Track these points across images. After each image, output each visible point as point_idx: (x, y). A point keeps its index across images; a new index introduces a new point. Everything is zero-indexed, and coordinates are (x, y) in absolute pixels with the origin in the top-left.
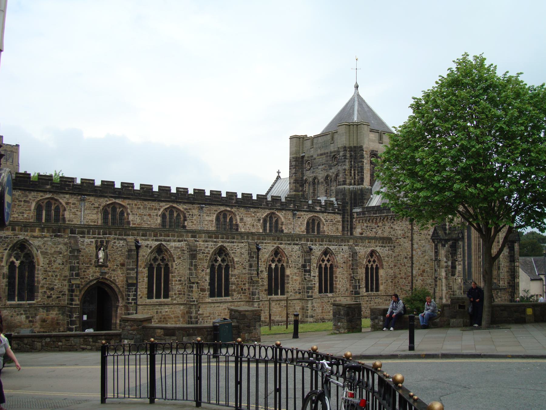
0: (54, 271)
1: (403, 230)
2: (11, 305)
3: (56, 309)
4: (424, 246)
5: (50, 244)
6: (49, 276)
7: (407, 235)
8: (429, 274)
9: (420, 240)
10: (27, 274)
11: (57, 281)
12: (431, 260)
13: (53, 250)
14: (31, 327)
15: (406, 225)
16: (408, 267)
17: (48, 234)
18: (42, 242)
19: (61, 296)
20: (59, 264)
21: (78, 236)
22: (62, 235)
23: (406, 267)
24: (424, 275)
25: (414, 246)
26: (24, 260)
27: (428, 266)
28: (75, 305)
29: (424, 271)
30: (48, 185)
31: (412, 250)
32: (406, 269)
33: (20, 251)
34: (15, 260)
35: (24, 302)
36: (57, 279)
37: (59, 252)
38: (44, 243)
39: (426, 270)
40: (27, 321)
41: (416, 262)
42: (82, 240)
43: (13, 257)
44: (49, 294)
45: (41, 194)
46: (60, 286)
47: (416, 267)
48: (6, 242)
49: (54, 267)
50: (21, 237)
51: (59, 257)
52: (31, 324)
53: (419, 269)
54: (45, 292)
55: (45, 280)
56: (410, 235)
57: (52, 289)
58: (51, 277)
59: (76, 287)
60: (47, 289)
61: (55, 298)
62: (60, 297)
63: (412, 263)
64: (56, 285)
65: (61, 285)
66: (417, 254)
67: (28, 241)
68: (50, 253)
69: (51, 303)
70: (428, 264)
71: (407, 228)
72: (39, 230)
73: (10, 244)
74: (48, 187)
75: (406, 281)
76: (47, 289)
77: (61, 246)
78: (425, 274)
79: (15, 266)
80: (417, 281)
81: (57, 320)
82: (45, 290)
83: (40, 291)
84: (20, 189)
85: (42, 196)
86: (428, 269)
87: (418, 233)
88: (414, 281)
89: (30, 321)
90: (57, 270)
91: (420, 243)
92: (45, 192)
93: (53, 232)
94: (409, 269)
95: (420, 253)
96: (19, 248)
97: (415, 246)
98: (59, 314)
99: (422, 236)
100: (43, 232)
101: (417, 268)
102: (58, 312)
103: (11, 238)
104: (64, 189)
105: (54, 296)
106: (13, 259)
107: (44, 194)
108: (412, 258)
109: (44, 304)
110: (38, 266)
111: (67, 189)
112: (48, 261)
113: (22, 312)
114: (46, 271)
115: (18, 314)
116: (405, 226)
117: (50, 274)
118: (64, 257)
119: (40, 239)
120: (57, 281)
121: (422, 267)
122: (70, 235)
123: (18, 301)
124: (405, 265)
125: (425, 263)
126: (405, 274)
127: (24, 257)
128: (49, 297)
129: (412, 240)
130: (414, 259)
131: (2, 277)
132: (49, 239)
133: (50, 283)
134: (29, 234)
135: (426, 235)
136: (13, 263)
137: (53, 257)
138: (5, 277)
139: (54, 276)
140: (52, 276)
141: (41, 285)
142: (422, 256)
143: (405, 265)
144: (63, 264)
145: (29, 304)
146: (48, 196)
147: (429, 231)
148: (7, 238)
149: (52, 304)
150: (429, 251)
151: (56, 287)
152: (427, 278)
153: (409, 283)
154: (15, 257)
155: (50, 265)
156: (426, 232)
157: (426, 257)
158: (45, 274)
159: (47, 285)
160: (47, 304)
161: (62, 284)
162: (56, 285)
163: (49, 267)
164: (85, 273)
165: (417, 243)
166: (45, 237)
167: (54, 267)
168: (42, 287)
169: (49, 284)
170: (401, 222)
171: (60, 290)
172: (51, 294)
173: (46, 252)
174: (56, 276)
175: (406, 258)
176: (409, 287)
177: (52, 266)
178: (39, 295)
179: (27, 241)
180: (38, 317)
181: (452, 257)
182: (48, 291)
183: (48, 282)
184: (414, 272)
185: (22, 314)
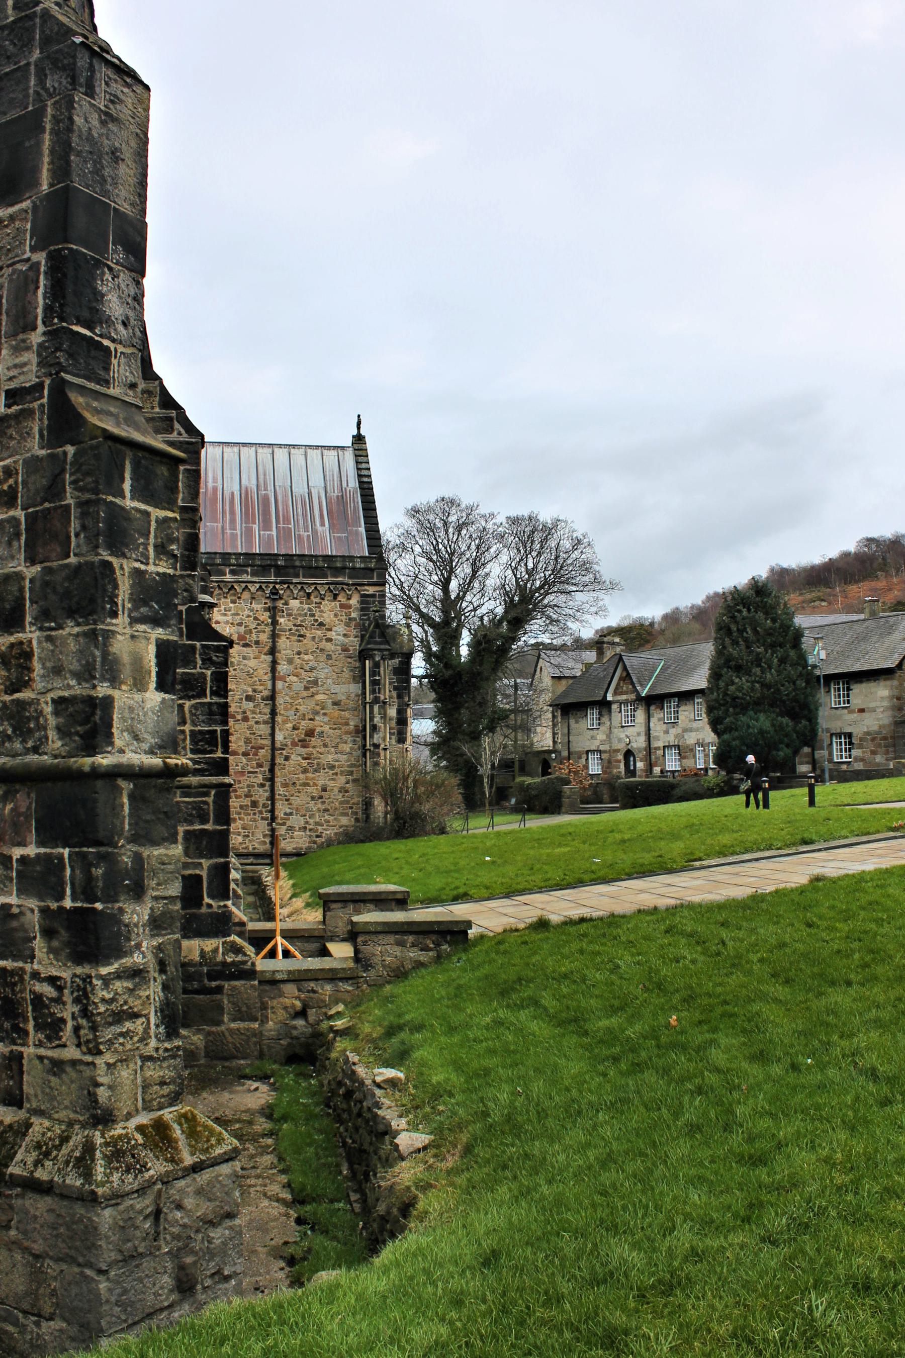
1: (240, 624)
4: (312, 669)
7: (254, 637)
8: (328, 740)
9: (299, 653)
12: (335, 703)
15: (252, 610)
16: (257, 723)
23: (252, 722)
24: (313, 743)
25: (279, 668)
27: (326, 719)
29: (310, 733)
31: (274, 679)
32: (250, 728)
39: (318, 729)
41: (286, 709)
47: (285, 722)
53: (295, 728)
56: (264, 637)
63: (273, 713)
66: (290, 687)
70: (325, 714)
71: (256, 619)
75: (249, 760)
78: (314, 741)
80: (287, 758)
86: (326, 728)
87: (294, 635)
88: (279, 760)
91: (299, 661)
94: (264, 729)
95: (298, 686)
97: (282, 668)
99: (305, 641)
101: (290, 725)
108: (272, 697)
116: (247, 612)
121: (303, 723)
124: (246, 719)
125: (317, 713)
126: (247, 741)
129: (273, 651)
130: (280, 700)
135: (321, 640)
142: (305, 694)
143: (246, 719)
147: (330, 630)
150: (329, 681)
152: (322, 750)
153: (260, 765)
156: (319, 632)
157: (320, 697)
165: (290, 661)
170: (233, 602)
175: (249, 698)
176: (260, 776)
181: (400, 696)
184: (279, 737)
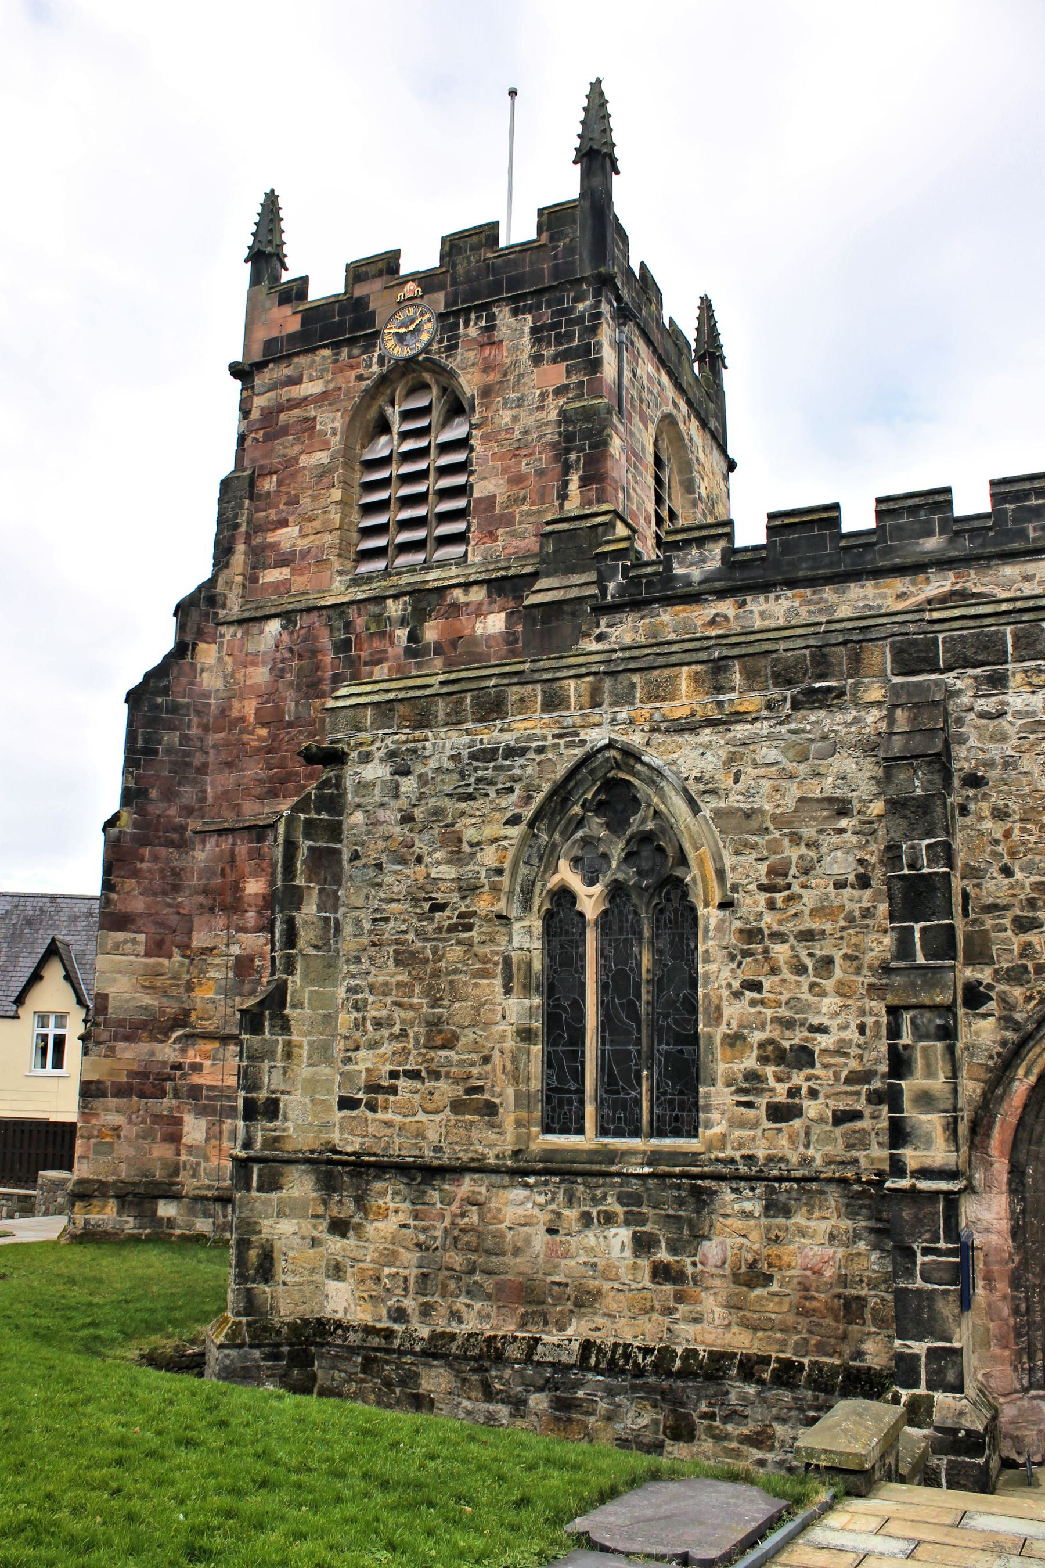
0: (807, 936)
2: (549, 1155)
3: (833, 1198)
5: (773, 755)
6: (774, 971)
10: (646, 960)
11: (830, 1003)
13: (794, 791)
14: (669, 1311)
17: (752, 702)
18: (723, 754)
19: (861, 1105)
20: (840, 885)
21: (961, 681)
22: (841, 693)
26: (628, 875)
28: (925, 1173)
30: (930, 534)
33: (608, 826)
34: (575, 881)
35: (636, 1143)
36: (829, 984)
37: (830, 800)
38: (732, 758)
40: (645, 1264)
42: (982, 704)
43: (564, 864)
44: (781, 1088)
45: (900, 584)
46: (852, 1034)
48: (516, 779)
49: (809, 899)
50: (597, 737)
51: (836, 839)
52: (669, 1288)
54: (752, 1076)
55: (749, 995)
57: (803, 1057)
58: (786, 973)
59: (919, 1034)
60: (764, 1060)
61: (821, 1120)
62: (857, 1115)
64: (822, 1029)
65: (862, 1029)
67: (638, 759)
68: (774, 818)
69: (794, 1159)
72: (696, 678)
73: (538, 789)
74: (932, 543)
76: (764, 1060)
77: (845, 763)
79: (581, 915)
81: (843, 1280)
82: (750, 1062)
83: (721, 1068)
84: (792, 584)
85: (901, 596)
89: (662, 1273)
90: (828, 927)
92: (916, 568)
93: (784, 679)
96: (600, 807)
98: (857, 1237)
100: (719, 689)
102: (846, 1224)
103: (541, 750)
104: (1022, 534)
105: (812, 1108)
106: (567, 875)
107: (914, 583)
109: (749, 1159)
110: (707, 905)
111: (1032, 534)
112: (763, 867)
113: (612, 1204)
114: (751, 935)
115: (586, 1220)
117: (781, 951)
118: (867, 831)
119: (706, 735)
120: (830, 1003)
122: (897, 680)
123: (603, 1131)
127: (629, 857)
128: (780, 1113)
131: (498, 982)
132: (763, 728)
133: (784, 1012)
134: (644, 710)
136: (564, 896)
137: (796, 839)
138: (515, 984)
139: (809, 963)
140: (800, 969)
141: (723, 1028)
144: (863, 882)
145: (654, 1158)
146: (940, 584)
148: (522, 752)
149: (806, 1161)
151: (825, 1041)
154: (576, 862)
155: (779, 897)
158: (746, 954)
159: (762, 1027)
160: (770, 1159)
161: (869, 1020)
162: (822, 1029)
163: (771, 906)
164: (1032, 937)
166: (738, 717)
167: (809, 899)
168: (735, 1040)
169: (777, 1020)
171: (854, 1065)
172: (793, 1092)
173: (748, 815)
174: (828, 962)
177: (789, 899)
178: (714, 1101)
179: (630, 755)
180: (712, 1250)
182: (770, 1070)
183: (769, 1013)
185: (608, 1219)
